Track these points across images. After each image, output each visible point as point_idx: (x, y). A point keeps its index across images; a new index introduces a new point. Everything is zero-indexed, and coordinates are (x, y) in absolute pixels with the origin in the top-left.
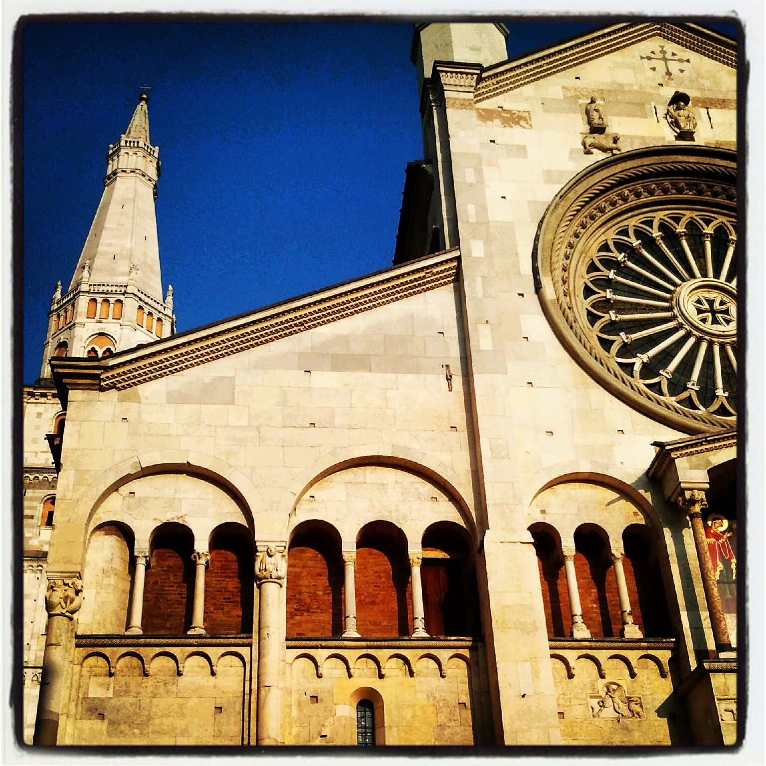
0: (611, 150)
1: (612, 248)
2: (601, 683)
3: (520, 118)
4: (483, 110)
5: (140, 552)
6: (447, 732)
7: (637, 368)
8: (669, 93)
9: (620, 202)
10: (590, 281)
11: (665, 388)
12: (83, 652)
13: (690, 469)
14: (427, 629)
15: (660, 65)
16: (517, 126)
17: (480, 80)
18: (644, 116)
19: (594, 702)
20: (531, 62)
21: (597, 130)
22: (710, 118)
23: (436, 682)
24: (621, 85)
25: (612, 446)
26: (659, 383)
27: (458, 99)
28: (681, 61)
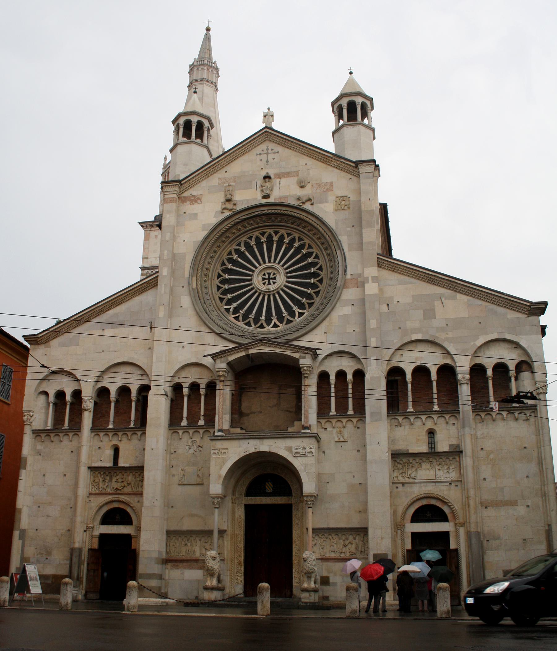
0: (232, 210)
1: (233, 253)
2: (190, 440)
3: (199, 199)
4: (184, 197)
5: (50, 401)
7: (231, 310)
8: (264, 173)
9: (237, 231)
10: (222, 271)
11: (241, 318)
13: (221, 363)
14: (135, 424)
15: (264, 157)
16: (196, 203)
17: (181, 185)
18: (251, 188)
19: (187, 447)
20: (205, 170)
21: (228, 200)
22: (280, 184)
25: (205, 351)
26: (239, 316)
27: (169, 198)
28: (274, 153)
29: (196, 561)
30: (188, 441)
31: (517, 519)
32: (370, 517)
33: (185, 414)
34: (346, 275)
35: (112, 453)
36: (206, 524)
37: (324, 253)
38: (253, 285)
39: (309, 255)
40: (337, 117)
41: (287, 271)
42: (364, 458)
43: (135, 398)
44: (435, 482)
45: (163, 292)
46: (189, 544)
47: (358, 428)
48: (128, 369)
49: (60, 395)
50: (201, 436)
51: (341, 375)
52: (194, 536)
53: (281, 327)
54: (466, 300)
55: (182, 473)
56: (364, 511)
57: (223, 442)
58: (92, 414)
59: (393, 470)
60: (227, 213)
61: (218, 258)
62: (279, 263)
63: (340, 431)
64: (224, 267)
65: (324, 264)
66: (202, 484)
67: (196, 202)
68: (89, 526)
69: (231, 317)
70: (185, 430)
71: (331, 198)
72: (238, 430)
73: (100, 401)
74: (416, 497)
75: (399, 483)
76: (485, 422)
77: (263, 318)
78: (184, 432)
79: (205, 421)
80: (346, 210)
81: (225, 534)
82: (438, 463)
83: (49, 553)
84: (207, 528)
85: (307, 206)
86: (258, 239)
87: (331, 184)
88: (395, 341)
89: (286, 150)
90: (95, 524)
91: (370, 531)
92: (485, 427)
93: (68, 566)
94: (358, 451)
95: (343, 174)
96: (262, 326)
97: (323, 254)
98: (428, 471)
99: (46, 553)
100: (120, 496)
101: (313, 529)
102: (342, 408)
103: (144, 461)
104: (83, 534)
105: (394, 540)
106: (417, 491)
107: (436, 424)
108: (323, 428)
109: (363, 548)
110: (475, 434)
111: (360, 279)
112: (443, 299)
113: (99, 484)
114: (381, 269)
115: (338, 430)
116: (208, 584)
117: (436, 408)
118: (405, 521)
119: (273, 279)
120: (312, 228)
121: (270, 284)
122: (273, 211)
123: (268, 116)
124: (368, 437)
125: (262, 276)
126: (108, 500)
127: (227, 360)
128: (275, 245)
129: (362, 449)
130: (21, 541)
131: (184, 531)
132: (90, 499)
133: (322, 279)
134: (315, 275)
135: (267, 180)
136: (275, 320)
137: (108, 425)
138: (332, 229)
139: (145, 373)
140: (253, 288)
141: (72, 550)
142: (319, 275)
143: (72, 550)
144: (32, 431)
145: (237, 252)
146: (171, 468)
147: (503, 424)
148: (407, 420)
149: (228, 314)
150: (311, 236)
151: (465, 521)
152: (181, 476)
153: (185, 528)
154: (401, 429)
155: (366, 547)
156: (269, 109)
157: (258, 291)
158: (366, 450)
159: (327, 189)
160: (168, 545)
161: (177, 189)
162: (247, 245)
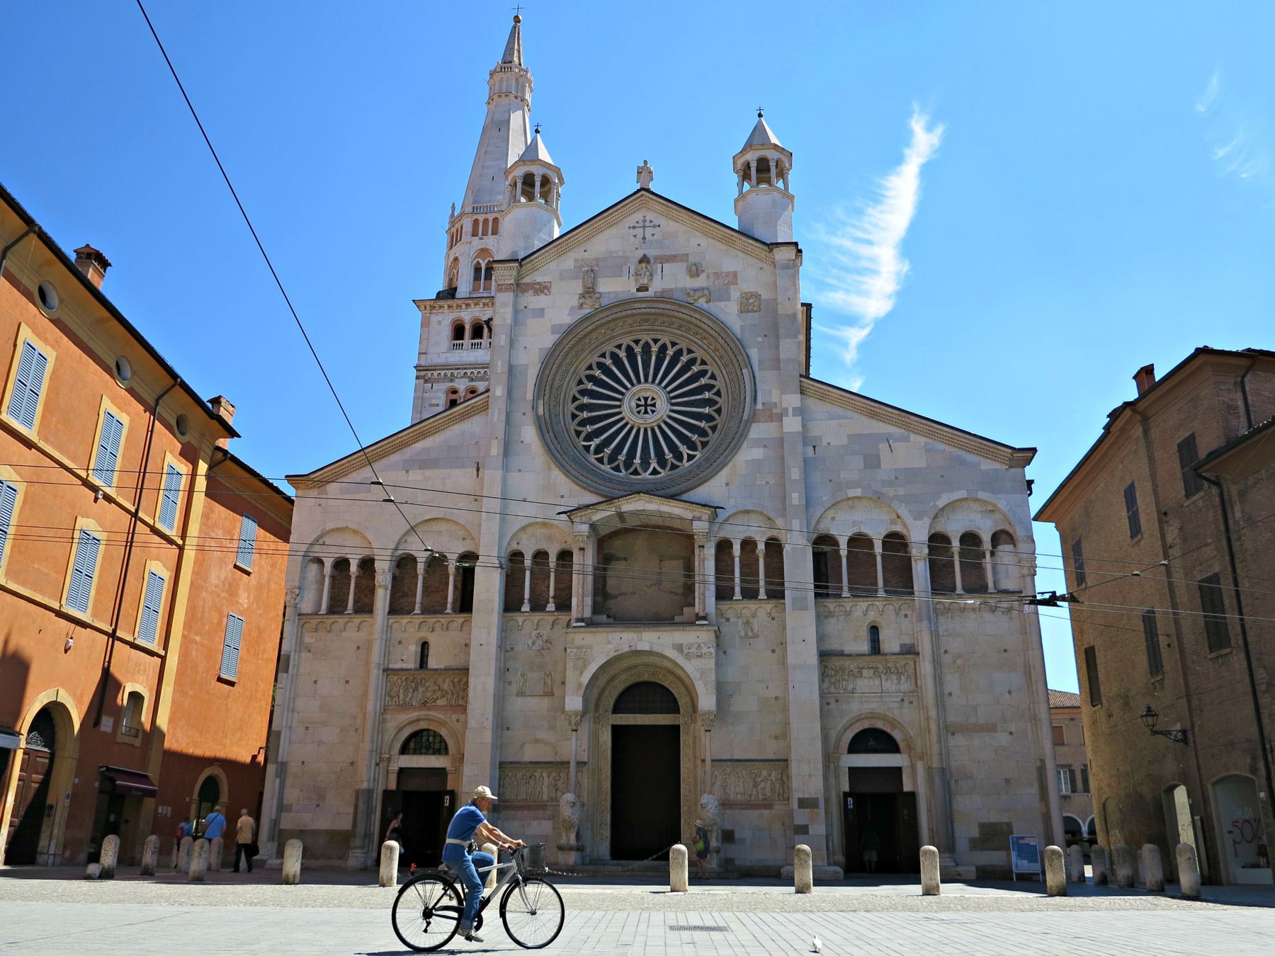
1: (594, 366)
2: (534, 633)
3: (546, 287)
4: (524, 284)
6: (458, 658)
8: (639, 254)
10: (579, 392)
11: (605, 460)
15: (639, 232)
17: (521, 266)
18: (621, 276)
19: (530, 642)
21: (589, 291)
24: (612, 252)
26: (603, 457)
28: (654, 226)
29: (543, 807)
30: (530, 634)
32: (793, 745)
33: (527, 596)
34: (755, 403)
35: (419, 649)
36: (556, 754)
37: (724, 371)
39: (703, 373)
40: (741, 178)
41: (673, 394)
42: (783, 662)
43: (453, 570)
45: (496, 420)
46: (532, 782)
48: (444, 527)
49: (342, 564)
51: (748, 545)
52: (539, 770)
53: (663, 473)
54: (923, 443)
55: (522, 680)
56: (783, 735)
57: (584, 635)
59: (823, 680)
60: (587, 311)
61: (573, 373)
62: (660, 383)
63: (748, 622)
67: (542, 292)
68: (383, 756)
69: (592, 458)
71: (735, 294)
72: (603, 618)
73: (401, 573)
77: (637, 461)
80: (755, 311)
81: (586, 767)
83: (322, 797)
84: (558, 760)
85: (702, 302)
87: (735, 274)
88: (824, 499)
89: (672, 223)
90: (392, 753)
91: (794, 768)
93: (351, 816)
94: (773, 651)
95: (752, 260)
96: (636, 472)
97: (722, 372)
98: (871, 680)
100: (431, 713)
101: (713, 761)
103: (468, 661)
104: (375, 769)
105: (826, 778)
111: (775, 411)
112: (891, 441)
113: (398, 695)
114: (804, 397)
116: (563, 841)
117: (881, 593)
119: (651, 405)
120: (707, 336)
121: (647, 413)
122: (653, 310)
123: (644, 171)
124: (789, 632)
126: (412, 719)
127: (591, 519)
129: (780, 647)
130: (278, 781)
131: (526, 763)
132: (385, 716)
134: (710, 402)
135: (644, 265)
137: (414, 610)
138: (737, 338)
140: (622, 419)
142: (716, 403)
143: (357, 792)
144: (299, 615)
145: (601, 366)
146: (507, 673)
148: (842, 608)
149: (587, 454)
150: (705, 347)
152: (521, 684)
153: (526, 759)
154: (833, 621)
156: (645, 162)
157: (631, 422)
158: (785, 649)
159: (729, 282)
160: (502, 783)
161: (514, 273)
162: (614, 356)
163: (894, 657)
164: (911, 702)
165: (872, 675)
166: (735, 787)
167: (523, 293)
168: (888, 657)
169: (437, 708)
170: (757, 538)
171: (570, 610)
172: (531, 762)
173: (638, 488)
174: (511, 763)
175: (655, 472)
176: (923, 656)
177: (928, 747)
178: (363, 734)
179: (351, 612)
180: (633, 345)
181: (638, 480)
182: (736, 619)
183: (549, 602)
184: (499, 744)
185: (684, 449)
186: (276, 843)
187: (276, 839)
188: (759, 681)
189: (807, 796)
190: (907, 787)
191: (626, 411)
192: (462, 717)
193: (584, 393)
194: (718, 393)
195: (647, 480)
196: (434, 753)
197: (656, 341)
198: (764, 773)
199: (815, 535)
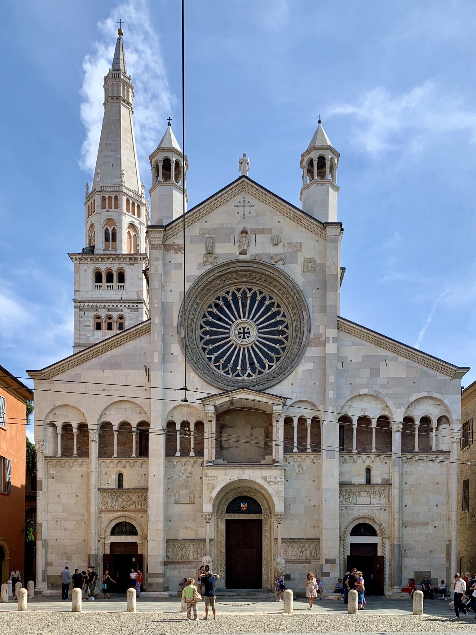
7: (213, 359)
10: (203, 322)
12: (47, 461)
19: (181, 474)
23: (138, 468)
31: (426, 536)
33: (178, 447)
38: (231, 338)
39: (278, 313)
41: (260, 326)
44: (370, 507)
47: (314, 463)
48: (127, 406)
50: (192, 465)
53: (254, 376)
55: (177, 495)
58: (97, 444)
61: (200, 310)
62: (252, 319)
64: (205, 319)
65: (290, 323)
66: (194, 503)
69: (213, 366)
70: (179, 460)
72: (221, 461)
74: (355, 517)
75: (343, 506)
76: (410, 463)
77: (239, 368)
78: (177, 461)
79: (195, 453)
82: (373, 493)
86: (234, 295)
92: (409, 466)
94: (313, 481)
96: (238, 375)
99: (66, 559)
102: (302, 448)
106: (356, 512)
107: (373, 462)
108: (287, 462)
109: (315, 553)
110: (402, 472)
115: (299, 464)
118: (346, 535)
119: (247, 333)
125: (238, 330)
128: (249, 301)
133: (287, 336)
134: (282, 332)
136: (249, 371)
139: (142, 411)
141: (89, 556)
142: (286, 333)
143: (89, 556)
145: (217, 305)
147: (423, 464)
151: (390, 535)
152: (177, 497)
155: (318, 553)
157: (235, 343)
162: (225, 299)
163: (378, 486)
164: (385, 510)
165: (365, 495)
166: (291, 552)
167: (167, 251)
168: (375, 486)
169: (130, 510)
170: (307, 416)
171: (203, 456)
172: (183, 539)
173: (240, 385)
174: (173, 540)
175: (249, 375)
176: (394, 487)
177: (393, 533)
178: (90, 524)
179: (76, 456)
180: (236, 292)
181: (240, 380)
182: (294, 463)
183: (191, 451)
184: (167, 530)
185: (266, 361)
186: (46, 582)
187: (46, 580)
188: (306, 497)
189: (329, 558)
190: (379, 554)
191: (232, 335)
192: (145, 515)
193: (207, 323)
194: (287, 327)
195: (245, 380)
196: (129, 535)
197: (250, 290)
198: (307, 545)
199: (340, 416)
